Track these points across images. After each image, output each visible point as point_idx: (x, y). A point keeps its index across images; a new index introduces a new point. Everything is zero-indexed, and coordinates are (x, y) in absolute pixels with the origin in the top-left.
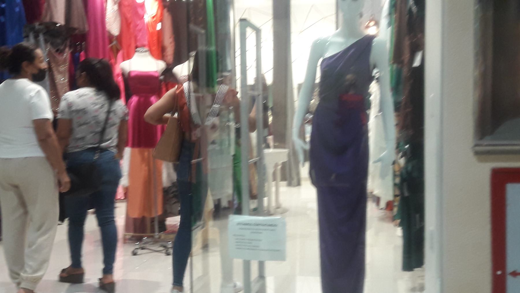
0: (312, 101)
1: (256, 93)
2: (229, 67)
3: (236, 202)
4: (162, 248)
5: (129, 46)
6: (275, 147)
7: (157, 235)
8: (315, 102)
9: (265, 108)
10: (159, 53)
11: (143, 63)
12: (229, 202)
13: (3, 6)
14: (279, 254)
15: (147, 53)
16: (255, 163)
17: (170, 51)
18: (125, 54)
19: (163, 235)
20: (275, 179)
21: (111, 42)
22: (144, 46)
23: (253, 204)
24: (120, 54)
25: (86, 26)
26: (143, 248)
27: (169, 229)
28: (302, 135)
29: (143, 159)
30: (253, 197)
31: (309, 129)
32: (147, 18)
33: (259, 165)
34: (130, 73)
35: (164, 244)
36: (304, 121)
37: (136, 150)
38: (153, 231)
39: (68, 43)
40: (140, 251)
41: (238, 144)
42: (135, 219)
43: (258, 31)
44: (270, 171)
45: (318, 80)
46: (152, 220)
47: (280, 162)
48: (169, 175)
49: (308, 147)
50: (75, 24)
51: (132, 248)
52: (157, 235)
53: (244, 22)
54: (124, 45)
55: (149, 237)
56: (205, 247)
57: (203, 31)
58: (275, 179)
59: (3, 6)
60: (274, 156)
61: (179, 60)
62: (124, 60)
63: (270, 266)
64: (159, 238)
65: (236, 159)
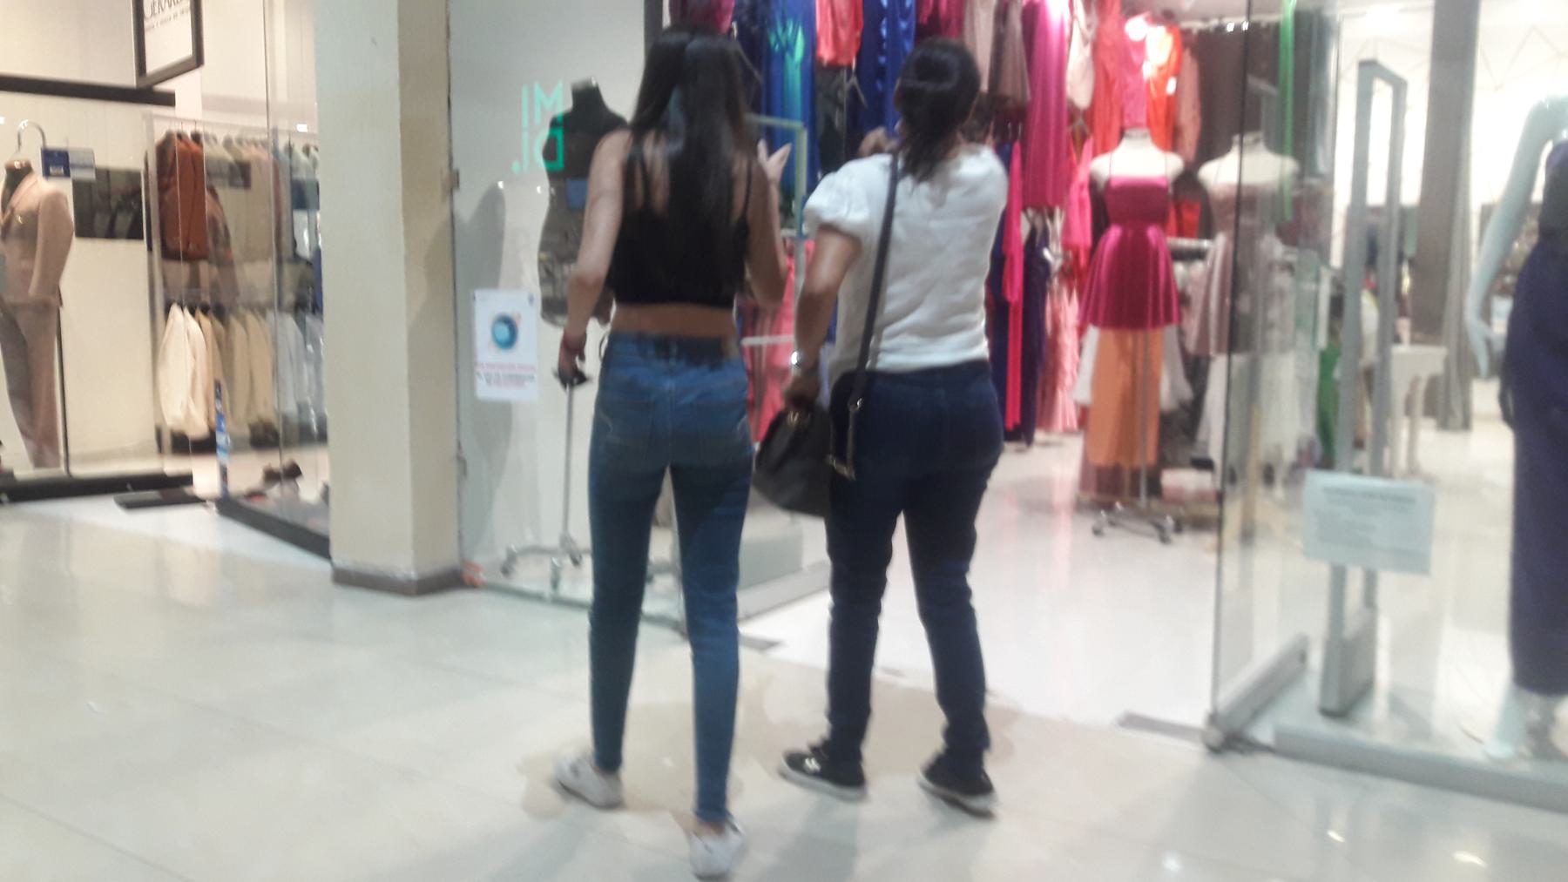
0: (1516, 245)
1: (1382, 221)
2: (1322, 167)
3: (1318, 451)
4: (1150, 529)
5: (1108, 127)
6: (1413, 341)
7: (1143, 501)
8: (1523, 246)
9: (1401, 257)
10: (1170, 139)
11: (1138, 160)
12: (1300, 452)
13: (882, 60)
14: (1414, 560)
15: (1148, 140)
16: (1369, 374)
17: (1190, 134)
18: (1099, 147)
19: (1155, 504)
20: (1409, 411)
21: (1072, 119)
22: (1136, 125)
23: (1363, 458)
24: (1088, 146)
25: (1028, 92)
26: (1112, 524)
27: (1166, 493)
28: (1486, 314)
29: (1123, 353)
30: (1359, 444)
31: (1503, 307)
32: (1149, 70)
33: (1373, 380)
34: (1108, 183)
35: (1158, 520)
36: (1494, 288)
37: (1111, 334)
38: (1135, 492)
39: (992, 127)
40: (1107, 530)
41: (1333, 332)
42: (1100, 471)
43: (1399, 86)
44: (1399, 392)
45: (1538, 196)
46: (1135, 474)
47: (1425, 375)
48: (1173, 387)
49: (1500, 345)
50: (1009, 87)
51: (1088, 522)
52: (1143, 501)
53: (1370, 69)
54: (1101, 126)
55: (1124, 504)
56: (1247, 535)
57: (1273, 91)
58: (1409, 411)
59: (882, 60)
60: (1414, 362)
61: (1209, 149)
62: (1095, 154)
63: (1389, 582)
64: (1148, 505)
65: (1326, 361)
